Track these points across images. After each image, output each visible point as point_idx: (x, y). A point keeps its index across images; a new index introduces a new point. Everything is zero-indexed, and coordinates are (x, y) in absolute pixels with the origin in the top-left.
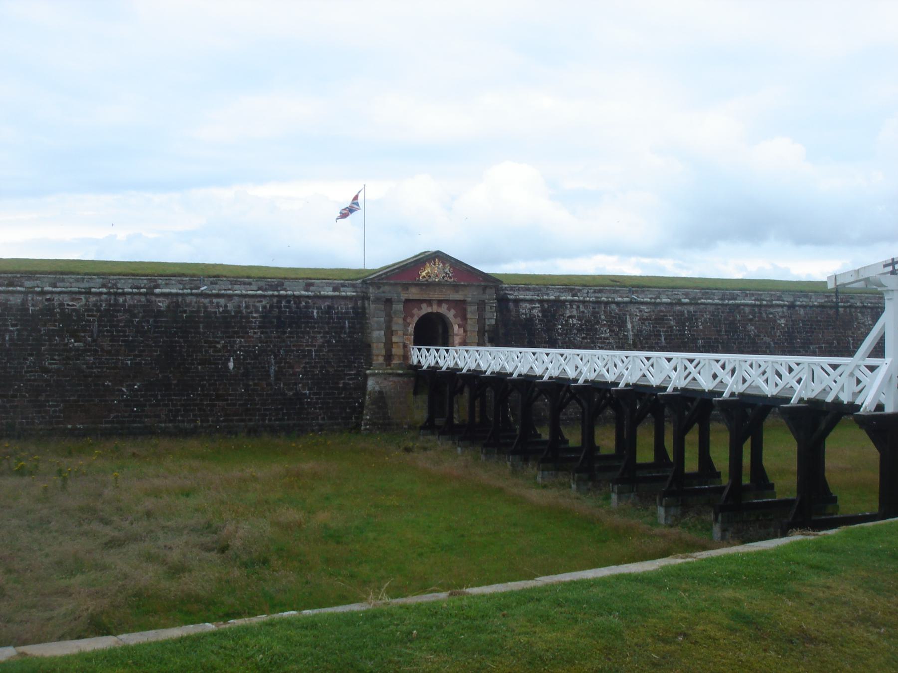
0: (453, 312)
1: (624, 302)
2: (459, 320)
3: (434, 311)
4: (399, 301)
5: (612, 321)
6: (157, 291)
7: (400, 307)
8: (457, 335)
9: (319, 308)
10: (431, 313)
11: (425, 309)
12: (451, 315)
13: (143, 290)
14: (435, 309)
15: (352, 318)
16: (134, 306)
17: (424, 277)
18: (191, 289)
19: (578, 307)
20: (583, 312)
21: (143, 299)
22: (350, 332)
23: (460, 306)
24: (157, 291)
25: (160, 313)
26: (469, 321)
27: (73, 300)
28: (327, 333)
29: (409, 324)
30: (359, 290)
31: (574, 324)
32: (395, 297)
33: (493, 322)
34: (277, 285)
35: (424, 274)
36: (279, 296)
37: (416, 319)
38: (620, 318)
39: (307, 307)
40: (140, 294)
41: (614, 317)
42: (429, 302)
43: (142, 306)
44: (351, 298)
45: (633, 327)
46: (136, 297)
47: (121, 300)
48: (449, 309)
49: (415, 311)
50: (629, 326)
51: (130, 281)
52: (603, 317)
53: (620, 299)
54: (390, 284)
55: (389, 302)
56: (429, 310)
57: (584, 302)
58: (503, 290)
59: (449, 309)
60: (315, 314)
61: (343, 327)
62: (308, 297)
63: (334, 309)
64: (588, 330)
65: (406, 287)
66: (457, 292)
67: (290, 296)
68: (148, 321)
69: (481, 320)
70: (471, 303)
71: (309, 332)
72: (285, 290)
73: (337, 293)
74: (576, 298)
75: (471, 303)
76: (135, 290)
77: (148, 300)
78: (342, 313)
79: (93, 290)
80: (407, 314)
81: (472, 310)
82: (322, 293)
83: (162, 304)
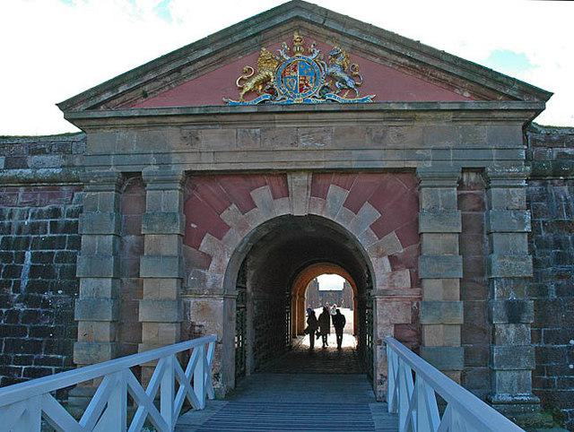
2: (393, 244)
3: (299, 211)
4: (165, 180)
7: (172, 198)
11: (268, 207)
12: (359, 226)
14: (299, 205)
15: (49, 243)
22: (30, 287)
26: (431, 244)
29: (209, 258)
33: (522, 243)
37: (236, 239)
44: (53, 182)
56: (282, 209)
70: (439, 178)
75: (439, 178)
80: (196, 223)
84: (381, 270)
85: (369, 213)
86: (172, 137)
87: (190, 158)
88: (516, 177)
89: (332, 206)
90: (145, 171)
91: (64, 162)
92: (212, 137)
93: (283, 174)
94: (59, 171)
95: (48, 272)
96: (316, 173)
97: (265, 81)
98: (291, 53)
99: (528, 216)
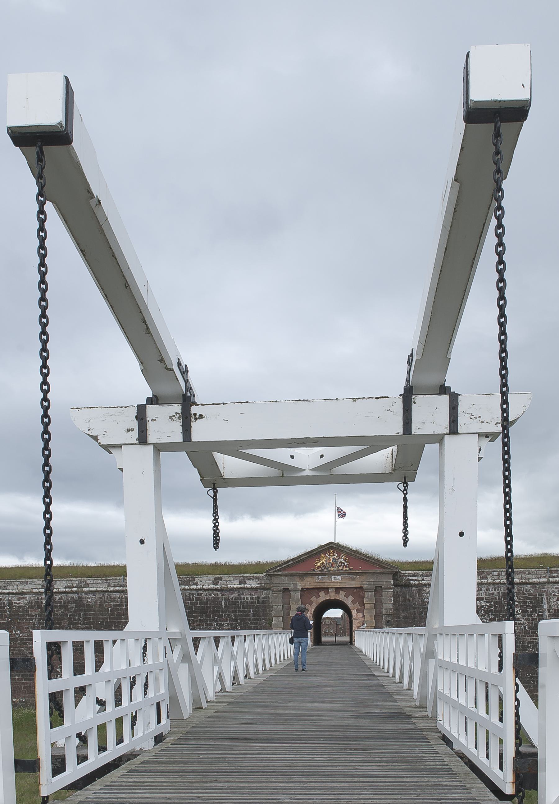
0: (351, 598)
1: (540, 583)
2: (357, 605)
4: (297, 590)
5: (525, 603)
6: (86, 589)
7: (298, 595)
8: (355, 619)
9: (225, 599)
10: (329, 599)
12: (349, 601)
13: (73, 589)
15: (257, 607)
16: (69, 602)
17: (319, 567)
18: (115, 586)
19: (488, 589)
20: (493, 593)
21: (76, 596)
22: (254, 619)
23: (358, 592)
24: (86, 589)
25: (89, 607)
27: (19, 599)
28: (234, 620)
29: (308, 610)
30: (263, 582)
31: (482, 606)
32: (292, 587)
33: (391, 606)
34: (189, 581)
35: (319, 564)
36: (190, 590)
37: (314, 606)
38: (535, 598)
39: (216, 598)
40: (73, 592)
41: (528, 598)
42: (326, 590)
43: (74, 602)
44: (256, 589)
45: (550, 607)
46: (71, 595)
47: (58, 598)
48: (347, 596)
49: (313, 599)
50: (546, 607)
51: (64, 582)
52: (516, 598)
53: (536, 580)
54: (286, 575)
55: (286, 590)
57: (493, 584)
58: (406, 576)
59: (347, 596)
60: (223, 604)
61: (248, 615)
62: (216, 589)
63: (241, 599)
64: (496, 611)
65: (303, 576)
66: (354, 579)
67: (200, 590)
68: (79, 615)
69: (378, 604)
71: (217, 621)
72: (196, 584)
73: (242, 586)
74: (485, 581)
76: (67, 590)
77: (80, 598)
78: (247, 603)
79: (34, 591)
81: (369, 595)
82: (229, 586)
83: (91, 600)
84: (354, 613)
85: (351, 598)
86: (297, 580)
87: (303, 585)
88: (391, 589)
89: (341, 596)
90: (290, 588)
91: (258, 582)
92: (309, 579)
93: (328, 588)
94: (259, 585)
95: (259, 615)
96: (336, 588)
97: (323, 563)
98: (329, 555)
99: (392, 599)
